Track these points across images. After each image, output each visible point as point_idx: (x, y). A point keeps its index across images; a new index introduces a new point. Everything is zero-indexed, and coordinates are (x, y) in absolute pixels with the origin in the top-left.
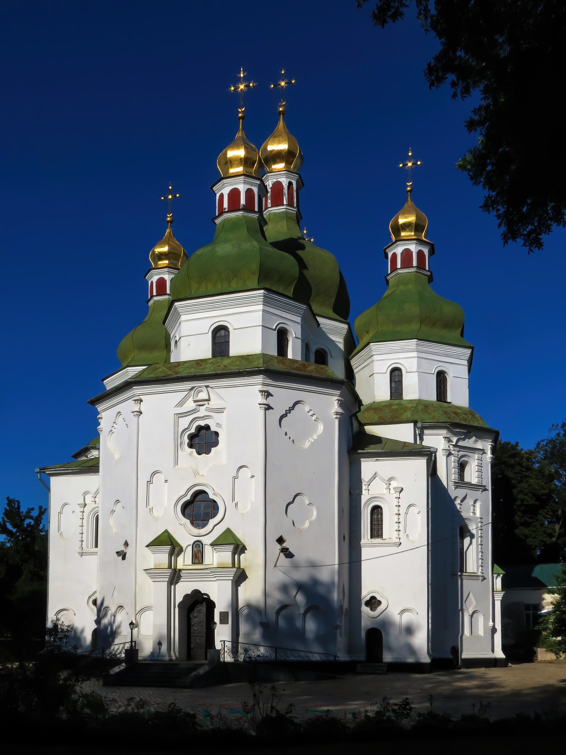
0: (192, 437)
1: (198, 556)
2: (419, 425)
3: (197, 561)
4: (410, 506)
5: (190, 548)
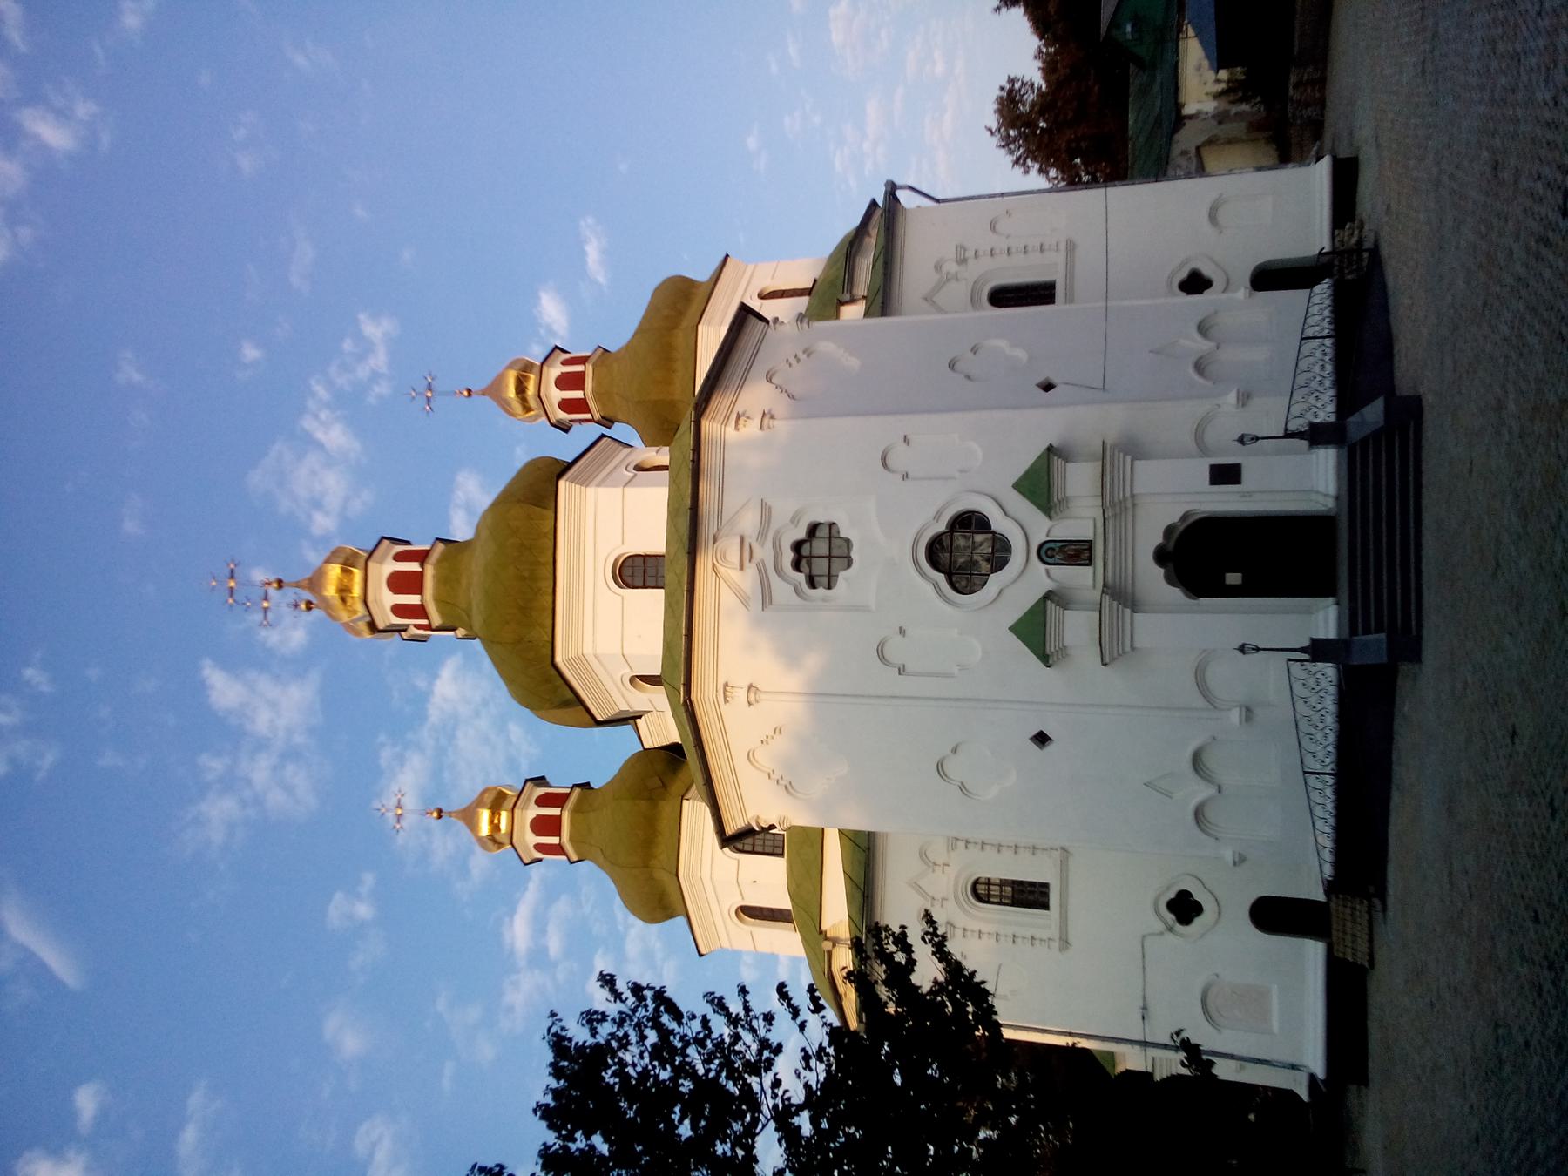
0: (812, 583)
1: (1075, 553)
2: (847, 297)
3: (1086, 554)
4: (993, 227)
5: (1056, 570)
